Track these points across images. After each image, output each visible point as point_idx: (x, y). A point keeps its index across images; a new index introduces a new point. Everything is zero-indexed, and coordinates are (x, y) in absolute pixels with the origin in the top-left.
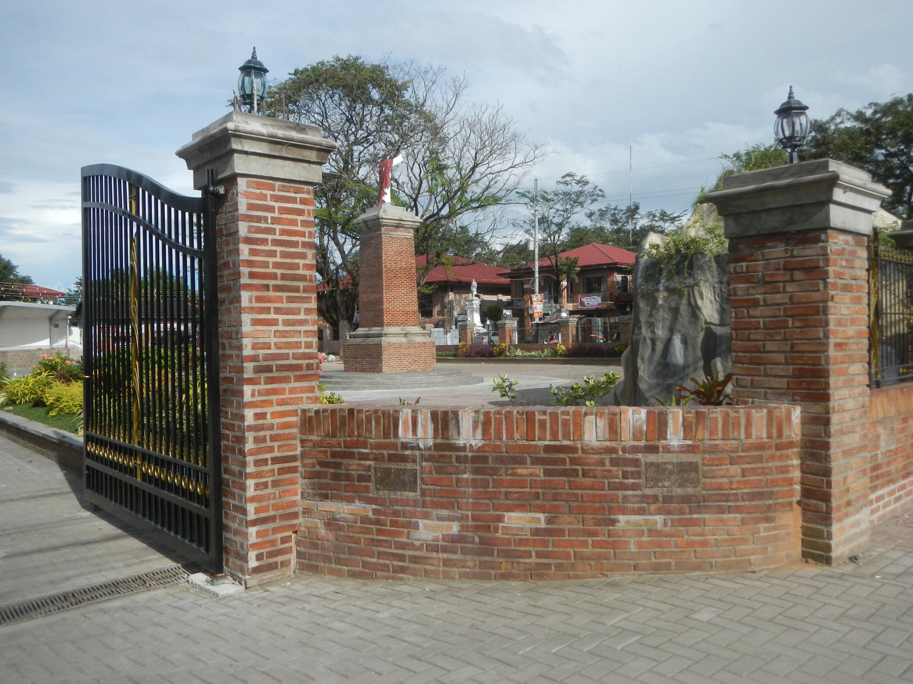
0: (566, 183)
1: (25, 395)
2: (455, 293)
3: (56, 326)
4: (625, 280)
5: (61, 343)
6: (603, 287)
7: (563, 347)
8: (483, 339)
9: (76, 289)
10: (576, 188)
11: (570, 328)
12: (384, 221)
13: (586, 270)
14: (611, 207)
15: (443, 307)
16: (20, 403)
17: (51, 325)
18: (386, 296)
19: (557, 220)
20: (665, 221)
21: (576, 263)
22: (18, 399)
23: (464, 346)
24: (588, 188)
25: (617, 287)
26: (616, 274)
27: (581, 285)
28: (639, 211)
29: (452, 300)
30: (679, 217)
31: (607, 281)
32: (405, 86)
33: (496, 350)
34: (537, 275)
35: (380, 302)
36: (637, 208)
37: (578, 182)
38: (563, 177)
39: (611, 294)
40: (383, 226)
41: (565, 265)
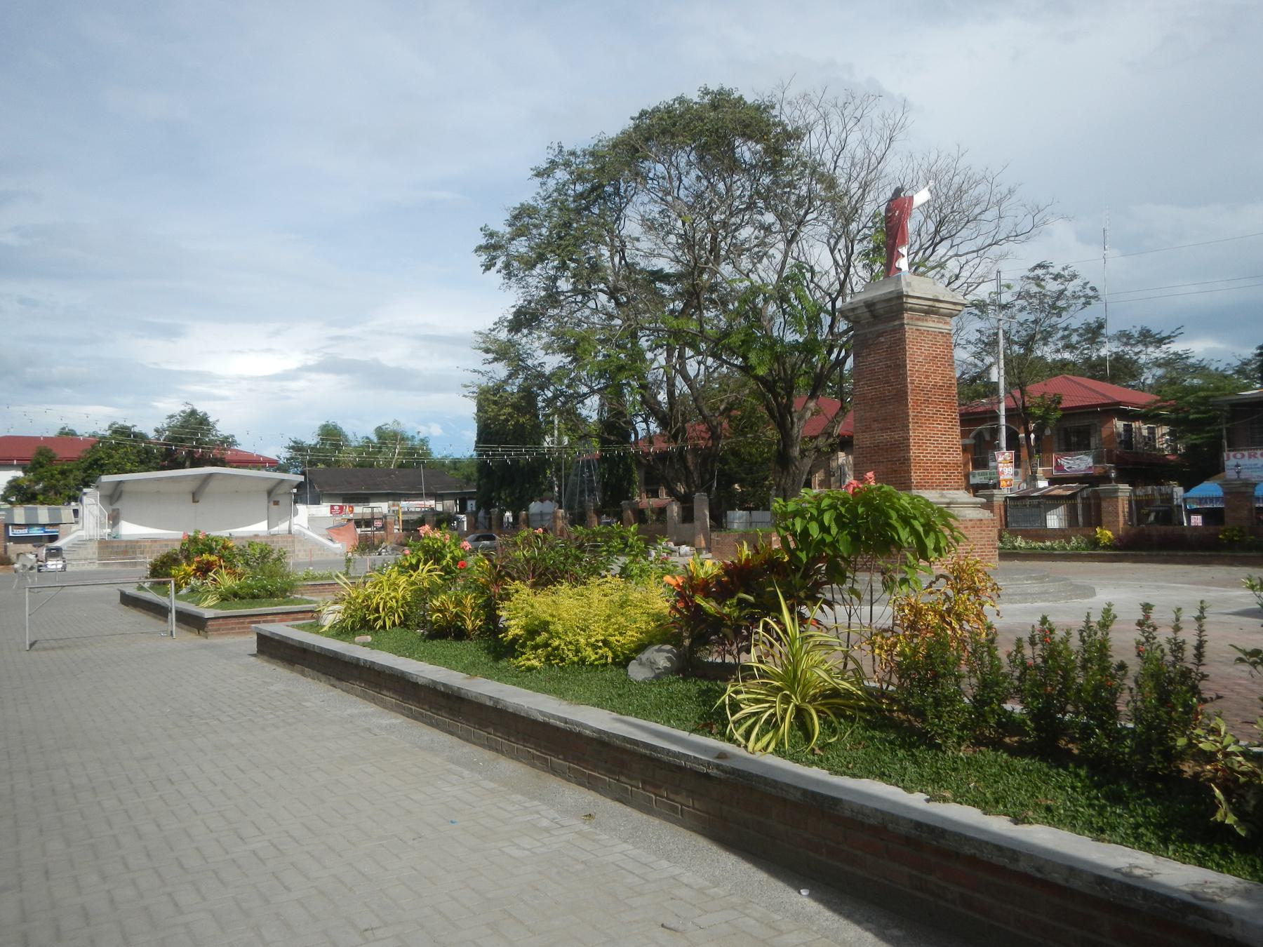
1: (392, 611)
2: (847, 454)
3: (276, 503)
4: (1128, 429)
5: (282, 527)
6: (1094, 442)
7: (1109, 533)
9: (288, 455)
10: (1052, 286)
11: (1120, 500)
12: (910, 300)
13: (1071, 413)
15: (829, 474)
16: (384, 627)
17: (269, 502)
18: (914, 434)
20: (1146, 346)
21: (1059, 403)
22: (376, 620)
24: (1072, 287)
25: (1118, 440)
28: (1104, 331)
29: (843, 465)
30: (1169, 337)
31: (1100, 431)
32: (797, 135)
34: (1003, 421)
35: (903, 445)
36: (1101, 326)
37: (1056, 277)
38: (1035, 268)
39: (1110, 451)
40: (907, 310)
41: (1039, 406)
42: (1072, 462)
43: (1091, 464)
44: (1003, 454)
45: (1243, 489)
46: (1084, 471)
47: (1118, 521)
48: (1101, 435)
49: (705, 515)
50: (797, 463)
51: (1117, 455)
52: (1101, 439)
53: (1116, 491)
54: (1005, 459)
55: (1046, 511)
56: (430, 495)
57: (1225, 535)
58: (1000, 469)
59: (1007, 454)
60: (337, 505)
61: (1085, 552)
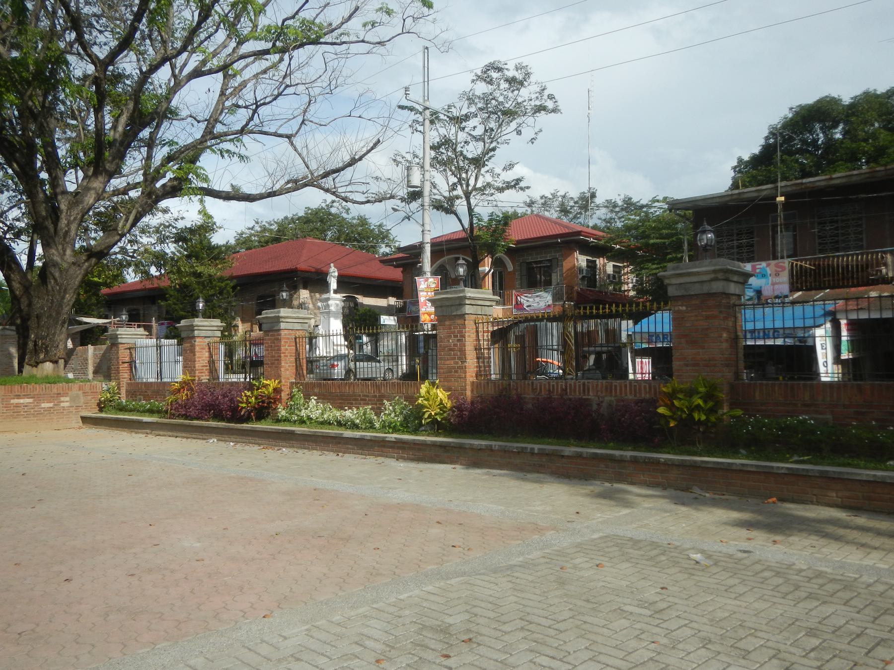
0: (490, 82)
4: (592, 266)
6: (555, 278)
7: (442, 394)
8: (333, 366)
11: (469, 324)
14: (559, 194)
19: (473, 150)
23: (185, 384)
25: (580, 276)
26: (577, 254)
27: (517, 276)
31: (562, 266)
36: (593, 196)
37: (511, 81)
39: (570, 288)
42: (530, 300)
43: (550, 302)
44: (427, 280)
45: (717, 287)
46: (544, 309)
47: (463, 369)
48: (562, 269)
49: (10, 356)
50: (57, 275)
52: (562, 275)
54: (428, 287)
57: (671, 407)
59: (431, 280)
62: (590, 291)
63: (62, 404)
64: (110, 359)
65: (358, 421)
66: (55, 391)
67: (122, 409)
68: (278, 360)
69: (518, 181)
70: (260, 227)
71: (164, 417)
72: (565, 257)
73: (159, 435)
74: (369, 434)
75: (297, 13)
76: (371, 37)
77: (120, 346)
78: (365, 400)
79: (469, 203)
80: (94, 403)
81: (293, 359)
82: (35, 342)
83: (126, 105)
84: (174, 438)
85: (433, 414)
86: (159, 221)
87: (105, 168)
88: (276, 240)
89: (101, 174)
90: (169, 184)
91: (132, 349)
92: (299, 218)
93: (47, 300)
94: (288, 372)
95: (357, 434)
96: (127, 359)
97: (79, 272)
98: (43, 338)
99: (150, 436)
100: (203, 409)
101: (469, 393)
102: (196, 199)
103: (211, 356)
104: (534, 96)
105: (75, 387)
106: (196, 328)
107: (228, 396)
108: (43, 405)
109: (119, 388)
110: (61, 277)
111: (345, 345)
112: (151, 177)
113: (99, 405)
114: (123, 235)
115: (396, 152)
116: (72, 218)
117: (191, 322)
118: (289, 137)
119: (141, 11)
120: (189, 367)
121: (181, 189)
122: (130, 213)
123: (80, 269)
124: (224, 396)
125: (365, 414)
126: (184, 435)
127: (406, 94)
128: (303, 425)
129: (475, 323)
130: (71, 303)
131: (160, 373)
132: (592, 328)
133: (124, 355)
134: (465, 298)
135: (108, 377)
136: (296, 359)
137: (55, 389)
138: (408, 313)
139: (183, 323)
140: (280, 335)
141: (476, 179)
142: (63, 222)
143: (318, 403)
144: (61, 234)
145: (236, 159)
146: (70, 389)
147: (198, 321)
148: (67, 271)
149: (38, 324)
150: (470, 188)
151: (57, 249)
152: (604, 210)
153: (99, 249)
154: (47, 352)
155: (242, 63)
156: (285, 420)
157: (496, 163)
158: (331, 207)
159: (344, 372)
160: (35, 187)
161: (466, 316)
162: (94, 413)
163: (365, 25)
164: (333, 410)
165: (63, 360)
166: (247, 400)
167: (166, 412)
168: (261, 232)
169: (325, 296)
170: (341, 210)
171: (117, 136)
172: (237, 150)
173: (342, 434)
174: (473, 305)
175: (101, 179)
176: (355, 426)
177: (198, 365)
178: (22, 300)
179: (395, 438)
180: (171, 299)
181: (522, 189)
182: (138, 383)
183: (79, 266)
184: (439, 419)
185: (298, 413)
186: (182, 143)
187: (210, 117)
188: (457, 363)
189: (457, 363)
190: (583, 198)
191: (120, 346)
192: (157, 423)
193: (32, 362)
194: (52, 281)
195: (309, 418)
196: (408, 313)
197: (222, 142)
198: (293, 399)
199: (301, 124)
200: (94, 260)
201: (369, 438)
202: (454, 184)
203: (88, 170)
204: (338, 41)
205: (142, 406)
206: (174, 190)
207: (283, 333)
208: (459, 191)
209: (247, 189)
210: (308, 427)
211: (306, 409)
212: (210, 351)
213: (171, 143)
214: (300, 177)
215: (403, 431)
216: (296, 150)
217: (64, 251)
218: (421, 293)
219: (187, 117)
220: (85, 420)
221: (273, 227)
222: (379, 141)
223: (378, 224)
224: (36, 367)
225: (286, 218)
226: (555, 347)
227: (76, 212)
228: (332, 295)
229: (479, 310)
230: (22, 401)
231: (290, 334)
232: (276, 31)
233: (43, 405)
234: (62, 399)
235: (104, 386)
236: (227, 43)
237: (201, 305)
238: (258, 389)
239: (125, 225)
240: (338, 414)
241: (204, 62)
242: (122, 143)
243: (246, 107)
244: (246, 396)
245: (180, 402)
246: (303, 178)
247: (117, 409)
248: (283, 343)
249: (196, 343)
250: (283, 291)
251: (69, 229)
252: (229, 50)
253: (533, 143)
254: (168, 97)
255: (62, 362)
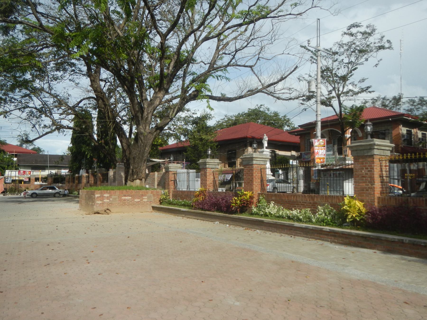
0: (352, 35)
4: (409, 133)
7: (359, 204)
11: (376, 160)
19: (342, 72)
23: (201, 192)
25: (403, 139)
26: (401, 126)
31: (392, 133)
33: (235, 201)
44: (319, 140)
47: (373, 189)
49: (121, 177)
50: (142, 138)
51: (401, 148)
53: (371, 147)
55: (343, 180)
56: (52, 167)
58: (316, 151)
59: (321, 141)
60: (22, 170)
61: (327, 228)
62: (409, 147)
63: (144, 200)
64: (165, 179)
65: (301, 217)
66: (141, 193)
67: (170, 203)
68: (252, 181)
69: (368, 87)
70: (227, 118)
71: (191, 209)
72: (393, 129)
73: (189, 218)
74: (310, 226)
75: (256, 3)
76: (296, 11)
77: (170, 172)
78: (304, 205)
79: (339, 101)
80: (158, 200)
81: (259, 181)
82: (133, 170)
83: (174, 56)
84: (196, 220)
85: (354, 216)
86: (186, 115)
87: (164, 87)
88: (235, 123)
89: (162, 90)
90: (193, 94)
91: (175, 174)
92: (245, 114)
93: (138, 150)
94: (257, 188)
95: (304, 225)
96: (173, 179)
97: (152, 137)
98: (136, 168)
99: (184, 218)
100: (211, 206)
101: (376, 204)
102: (204, 100)
103: (214, 178)
104: (377, 41)
105: (150, 191)
106: (207, 164)
107: (224, 199)
108: (136, 200)
109: (169, 193)
110: (144, 139)
111: (271, 175)
112: (184, 90)
113: (160, 201)
114: (171, 119)
115: (300, 75)
116: (149, 111)
117: (204, 160)
118: (251, 67)
119: (182, 7)
120: (203, 184)
121: (197, 96)
122: (175, 108)
123: (152, 136)
124: (223, 199)
125: (305, 213)
126: (201, 218)
127: (308, 44)
128: (267, 217)
129: (380, 161)
130: (148, 152)
131: (188, 186)
132: (421, 167)
133: (171, 177)
134: (375, 145)
135: (164, 188)
136: (261, 181)
137: (141, 192)
138: (303, 159)
139: (201, 161)
140: (253, 167)
141: (343, 87)
142: (145, 113)
143: (274, 205)
144: (144, 119)
145: (224, 80)
146: (147, 193)
147: (208, 160)
148: (147, 136)
149: (134, 161)
150: (340, 92)
151: (142, 126)
152: (407, 105)
153: (161, 125)
154: (137, 175)
155: (230, 31)
156: (256, 214)
157: (356, 77)
158: (261, 108)
159: (272, 188)
160: (134, 97)
161: (375, 156)
162: (157, 205)
163: (291, 6)
164: (284, 210)
165: (144, 179)
166: (236, 202)
167: (192, 206)
168: (227, 121)
169: (262, 150)
170: (265, 109)
171: (169, 72)
172: (224, 75)
173: (293, 224)
174: (378, 149)
175: (162, 92)
176: (299, 220)
177: (208, 183)
178: (127, 151)
179: (329, 230)
180: (189, 151)
181: (370, 92)
182: (178, 191)
183: (152, 134)
184: (358, 220)
185: (264, 210)
186: (199, 73)
187: (212, 61)
188: (368, 185)
189: (368, 185)
190: (394, 98)
191: (170, 172)
192: (188, 212)
193: (131, 179)
194: (140, 141)
195: (270, 214)
196: (303, 159)
197: (217, 71)
198: (261, 202)
199: (257, 60)
200: (158, 131)
201: (311, 228)
202: (331, 91)
203: (156, 89)
204: (276, 16)
205: (180, 202)
206: (195, 97)
207: (254, 166)
208: (334, 94)
209: (229, 96)
210: (270, 219)
211: (268, 208)
212: (214, 176)
213: (193, 74)
214: (254, 89)
215: (333, 225)
216: (254, 73)
217: (146, 127)
218: (316, 148)
219: (200, 62)
220: (154, 208)
221: (233, 118)
222: (297, 67)
223: (283, 115)
224: (133, 182)
225: (239, 114)
226: (396, 177)
227: (151, 108)
228: (265, 149)
229: (381, 152)
230: (126, 198)
231: (258, 167)
232: (245, 14)
233: (136, 200)
234: (144, 197)
235: (162, 192)
236: (220, 22)
237: (210, 152)
238: (241, 196)
239: (172, 114)
240: (288, 212)
241: (210, 33)
242: (171, 75)
243: (229, 54)
244: (235, 200)
245: (199, 201)
246: (255, 89)
247: (168, 203)
248: (254, 172)
249: (207, 171)
250: (254, 144)
251: (148, 117)
252: (220, 28)
253: (376, 66)
254: (193, 52)
255: (143, 180)
